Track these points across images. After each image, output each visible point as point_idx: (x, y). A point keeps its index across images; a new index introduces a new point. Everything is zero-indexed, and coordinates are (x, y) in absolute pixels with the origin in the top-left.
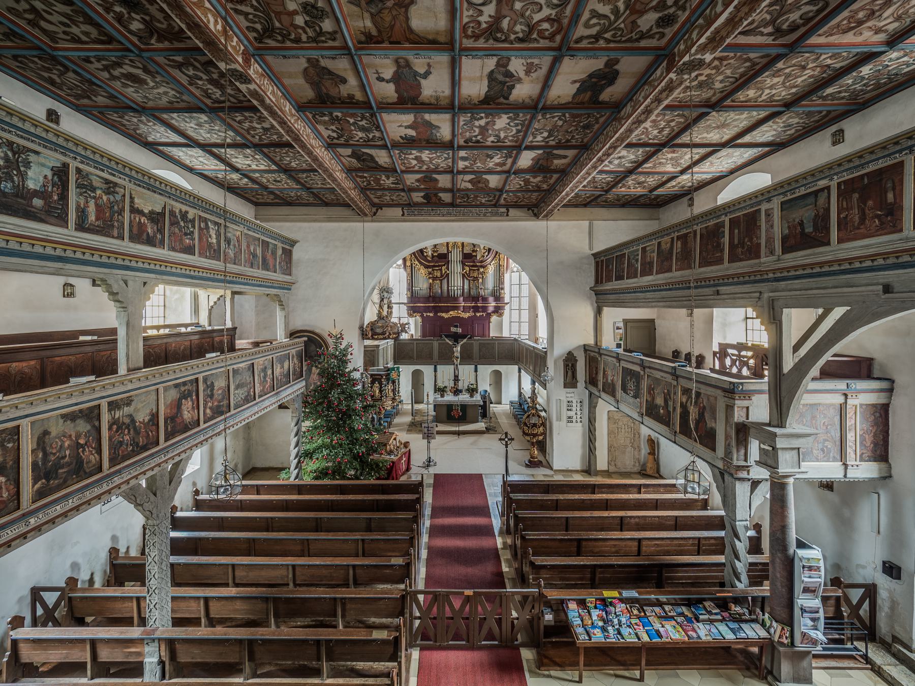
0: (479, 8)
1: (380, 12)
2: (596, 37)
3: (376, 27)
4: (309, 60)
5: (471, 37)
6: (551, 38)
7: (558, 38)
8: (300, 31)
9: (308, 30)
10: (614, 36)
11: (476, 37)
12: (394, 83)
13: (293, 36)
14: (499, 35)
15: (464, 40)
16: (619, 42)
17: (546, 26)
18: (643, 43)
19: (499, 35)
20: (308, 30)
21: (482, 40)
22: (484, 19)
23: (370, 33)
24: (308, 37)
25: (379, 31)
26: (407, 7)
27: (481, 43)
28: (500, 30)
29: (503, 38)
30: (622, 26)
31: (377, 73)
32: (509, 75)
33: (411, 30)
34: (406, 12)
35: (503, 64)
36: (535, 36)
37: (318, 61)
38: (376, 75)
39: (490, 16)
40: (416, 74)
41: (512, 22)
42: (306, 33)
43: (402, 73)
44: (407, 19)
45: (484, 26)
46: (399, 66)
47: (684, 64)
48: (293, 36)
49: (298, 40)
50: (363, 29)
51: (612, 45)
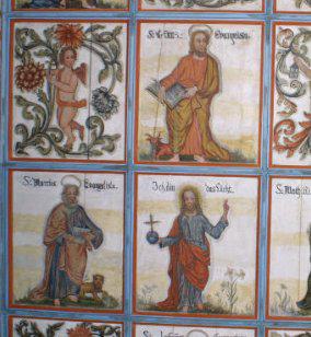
0: (292, 100)
1: (178, 104)
3: (169, 129)
8: (76, 133)
9: (86, 131)
11: (290, 148)
12: (171, 251)
13: (62, 144)
15: (275, 155)
20: (86, 131)
21: (297, 155)
22: (298, 117)
23: (159, 139)
25: (171, 136)
26: (210, 97)
27: (296, 159)
31: (151, 222)
33: (210, 138)
34: (209, 103)
37: (77, 192)
38: (147, 228)
39: (305, 114)
40: (205, 225)
42: (82, 138)
44: (208, 115)
45: (299, 129)
46: (184, 208)
48: (62, 144)
49: (66, 151)
50: (151, 133)
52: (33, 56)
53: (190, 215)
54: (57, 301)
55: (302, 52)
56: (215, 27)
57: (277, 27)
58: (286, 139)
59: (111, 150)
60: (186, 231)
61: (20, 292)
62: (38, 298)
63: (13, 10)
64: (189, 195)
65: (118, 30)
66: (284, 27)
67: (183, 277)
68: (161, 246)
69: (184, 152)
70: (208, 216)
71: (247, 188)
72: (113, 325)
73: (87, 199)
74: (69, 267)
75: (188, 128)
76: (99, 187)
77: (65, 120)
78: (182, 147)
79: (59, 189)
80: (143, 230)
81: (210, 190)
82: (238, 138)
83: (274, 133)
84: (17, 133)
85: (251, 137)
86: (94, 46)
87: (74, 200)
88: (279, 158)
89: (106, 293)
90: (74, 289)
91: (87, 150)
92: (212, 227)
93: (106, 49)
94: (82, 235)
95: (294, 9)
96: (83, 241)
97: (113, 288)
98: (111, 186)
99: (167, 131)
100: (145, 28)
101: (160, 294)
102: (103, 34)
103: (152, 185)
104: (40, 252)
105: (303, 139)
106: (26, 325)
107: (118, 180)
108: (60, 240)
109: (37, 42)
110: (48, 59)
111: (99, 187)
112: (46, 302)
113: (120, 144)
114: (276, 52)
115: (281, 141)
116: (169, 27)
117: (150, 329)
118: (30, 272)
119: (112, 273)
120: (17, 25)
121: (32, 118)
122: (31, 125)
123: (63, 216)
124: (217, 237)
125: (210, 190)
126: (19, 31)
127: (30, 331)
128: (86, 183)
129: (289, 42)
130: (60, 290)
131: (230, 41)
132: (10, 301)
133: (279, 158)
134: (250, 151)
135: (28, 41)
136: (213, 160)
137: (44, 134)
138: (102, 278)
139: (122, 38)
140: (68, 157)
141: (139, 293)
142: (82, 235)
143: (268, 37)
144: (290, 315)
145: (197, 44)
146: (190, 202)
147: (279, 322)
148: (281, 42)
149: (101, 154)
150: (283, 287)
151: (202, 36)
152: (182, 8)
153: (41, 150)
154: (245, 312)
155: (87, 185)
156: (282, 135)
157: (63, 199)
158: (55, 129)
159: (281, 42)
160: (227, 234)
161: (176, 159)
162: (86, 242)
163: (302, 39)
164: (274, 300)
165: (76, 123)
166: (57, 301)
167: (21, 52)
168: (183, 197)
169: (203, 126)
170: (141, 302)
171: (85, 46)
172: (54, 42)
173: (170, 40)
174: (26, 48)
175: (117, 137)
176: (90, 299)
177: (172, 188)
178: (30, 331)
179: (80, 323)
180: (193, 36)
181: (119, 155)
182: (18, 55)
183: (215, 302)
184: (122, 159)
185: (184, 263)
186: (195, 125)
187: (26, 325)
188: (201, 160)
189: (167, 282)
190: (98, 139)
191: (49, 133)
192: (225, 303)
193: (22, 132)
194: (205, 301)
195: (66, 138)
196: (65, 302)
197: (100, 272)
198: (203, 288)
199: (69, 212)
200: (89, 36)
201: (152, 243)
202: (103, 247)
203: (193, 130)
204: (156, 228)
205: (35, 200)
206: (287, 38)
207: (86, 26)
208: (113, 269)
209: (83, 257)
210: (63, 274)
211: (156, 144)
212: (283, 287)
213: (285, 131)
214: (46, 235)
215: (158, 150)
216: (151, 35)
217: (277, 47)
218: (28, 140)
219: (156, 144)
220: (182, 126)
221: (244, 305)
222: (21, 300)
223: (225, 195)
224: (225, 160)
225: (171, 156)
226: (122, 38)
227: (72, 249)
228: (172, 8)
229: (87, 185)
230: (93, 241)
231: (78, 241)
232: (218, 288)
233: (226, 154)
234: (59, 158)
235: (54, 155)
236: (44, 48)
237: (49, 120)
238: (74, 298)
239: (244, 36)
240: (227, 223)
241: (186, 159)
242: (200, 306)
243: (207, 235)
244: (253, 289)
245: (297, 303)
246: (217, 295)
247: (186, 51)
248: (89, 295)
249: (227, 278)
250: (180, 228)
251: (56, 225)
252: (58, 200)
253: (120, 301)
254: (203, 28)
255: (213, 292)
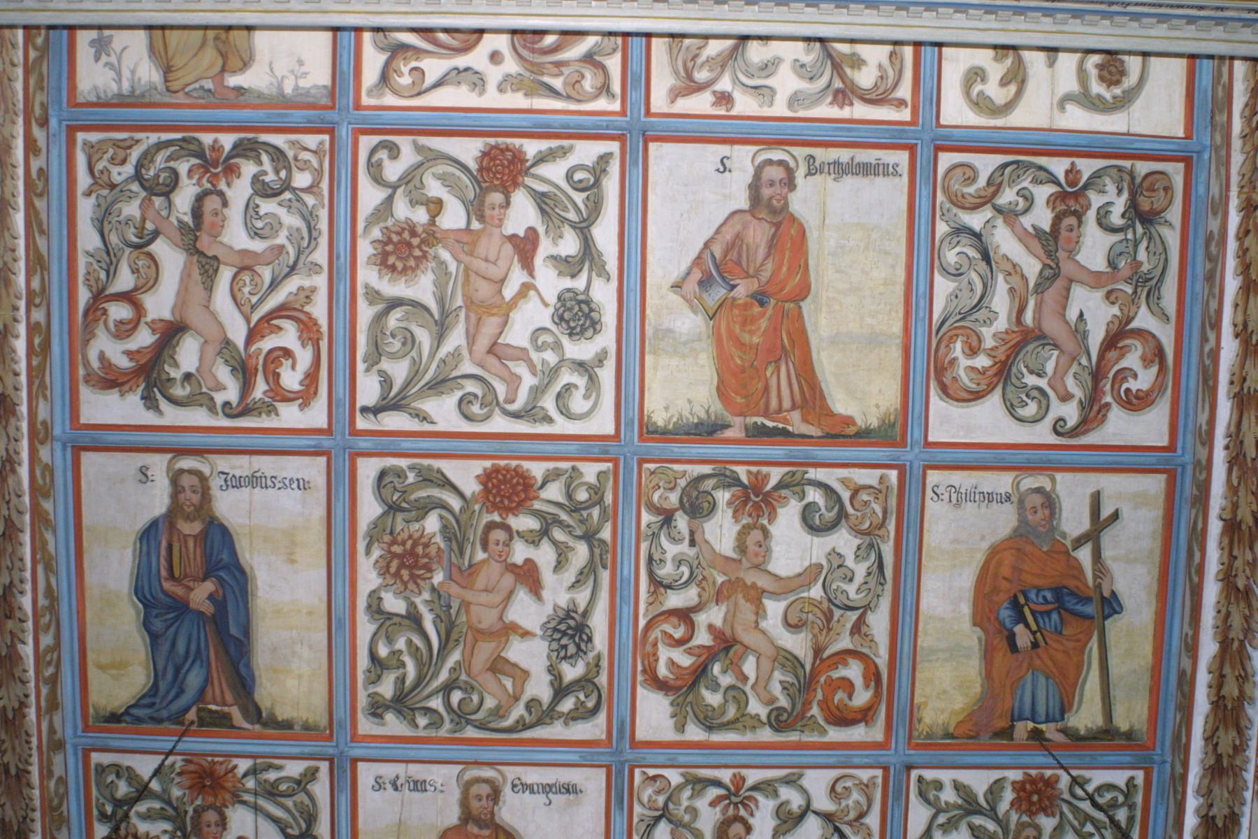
52: (134, 820)
55: (687, 818)
56: (511, 773)
57: (637, 772)
63: (87, 728)
65: (312, 774)
66: (652, 772)
86: (262, 802)
93: (287, 810)
95: (670, 736)
100: (366, 774)
102: (279, 781)
109: (143, 792)
110: (168, 826)
114: (635, 820)
116: (416, 770)
120: (96, 758)
126: (101, 770)
129: (661, 800)
131: (541, 799)
135: (123, 789)
139: (320, 789)
143: (618, 795)
145: (475, 804)
148: (645, 799)
151: (485, 789)
152: (443, 733)
159: (645, 799)
163: (687, 793)
167: (109, 809)
171: (244, 803)
172: (176, 792)
173: (416, 795)
174: (118, 803)
180: (466, 787)
182: (104, 817)
200: (250, 783)
206: (659, 792)
207: (243, 765)
216: (379, 785)
217: (638, 809)
226: (320, 789)
228: (422, 734)
236: (157, 805)
239: (570, 789)
247: (452, 816)
254: (488, 773)
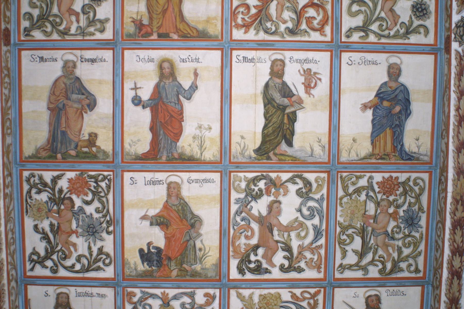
2: (364, 29)
3: (149, 12)
4: (66, 63)
5: (243, 26)
6: (321, 30)
7: (328, 29)
8: (73, 18)
9: (81, 16)
10: (381, 26)
11: (246, 26)
14: (269, 25)
15: (235, 31)
16: (388, 37)
17: (311, 12)
18: (414, 39)
19: (269, 25)
20: (81, 16)
21: (252, 31)
23: (141, 21)
24: (79, 28)
25: (151, 18)
27: (251, 35)
28: (269, 18)
29: (274, 29)
30: (383, 15)
31: (136, 88)
32: (286, 92)
35: (277, 70)
36: (304, 26)
37: (75, 66)
38: (132, 93)
41: (280, 7)
42: (78, 21)
43: (164, 87)
45: (253, 11)
46: (162, 76)
47: (457, 26)
49: (66, 32)
50: (135, 16)
51: (383, 40)
53: (167, 82)
54: (59, 156)
58: (243, 19)
59: (102, 31)
60: (164, 95)
61: (28, 150)
62: (44, 154)
64: (166, 65)
67: (162, 132)
68: (144, 107)
69: (161, 31)
70: (181, 82)
71: (212, 59)
72: (106, 173)
73: (84, 72)
74: (68, 127)
75: (164, 12)
76: (93, 61)
77: (64, 8)
78: (159, 28)
79: (60, 64)
80: (129, 94)
81: (183, 61)
82: (205, 18)
83: (234, 14)
84: (25, 20)
85: (215, 18)
87: (72, 73)
88: (238, 34)
89: (99, 148)
90: (73, 146)
91: (82, 31)
92: (185, 91)
94: (80, 101)
96: (80, 106)
97: (105, 143)
98: (102, 60)
99: (147, 14)
101: (144, 147)
103: (135, 58)
104: (45, 116)
105: (256, 20)
106: (34, 176)
107: (108, 55)
108: (61, 106)
111: (93, 61)
112: (50, 157)
113: (109, 26)
115: (239, 21)
117: (136, 175)
118: (36, 131)
119: (104, 131)
121: (36, 7)
122: (36, 13)
123: (63, 85)
124: (189, 99)
125: (183, 61)
127: (37, 181)
128: (81, 58)
130: (62, 145)
132: (21, 158)
133: (238, 34)
134: (215, 29)
136: (185, 37)
137: (47, 19)
138: (96, 135)
140: (67, 38)
141: (126, 146)
142: (80, 101)
144: (248, 161)
146: (167, 71)
147: (240, 166)
149: (93, 34)
150: (242, 137)
153: (45, 32)
154: (212, 159)
155: (83, 60)
156: (240, 16)
157: (63, 71)
158: (56, 16)
160: (197, 96)
161: (155, 36)
162: (83, 106)
164: (235, 149)
165: (74, 10)
166: (59, 156)
168: (161, 67)
169: (176, 10)
170: (128, 154)
175: (107, 20)
176: (86, 153)
177: (152, 60)
178: (37, 181)
179: (78, 173)
181: (108, 35)
183: (188, 151)
184: (111, 38)
185: (163, 121)
186: (171, 9)
187: (34, 176)
188: (175, 37)
189: (149, 136)
190: (91, 22)
191: (51, 19)
192: (196, 152)
193: (29, 19)
194: (179, 151)
195: (65, 23)
196: (65, 156)
197: (95, 131)
198: (178, 140)
199: (68, 83)
201: (136, 105)
202: (96, 109)
203: (168, 15)
204: (140, 93)
205: (39, 74)
208: (105, 128)
209: (80, 119)
210: (64, 133)
211: (139, 25)
212: (242, 137)
213: (242, 12)
214: (50, 102)
215: (140, 30)
218: (33, 25)
219: (139, 25)
220: (160, 10)
221: (211, 153)
222: (30, 157)
223: (194, 65)
224: (195, 36)
225: (151, 34)
227: (71, 112)
229: (83, 60)
230: (89, 105)
231: (76, 105)
232: (190, 140)
233: (195, 31)
234: (60, 38)
235: (55, 36)
237: (51, 9)
238: (73, 153)
240: (197, 87)
241: (163, 36)
242: (176, 156)
243: (181, 97)
244: (218, 140)
245: (254, 151)
246: (190, 145)
248: (86, 150)
249: (198, 132)
250: (159, 93)
251: (57, 93)
252: (59, 73)
253: (111, 152)
255: (186, 144)
